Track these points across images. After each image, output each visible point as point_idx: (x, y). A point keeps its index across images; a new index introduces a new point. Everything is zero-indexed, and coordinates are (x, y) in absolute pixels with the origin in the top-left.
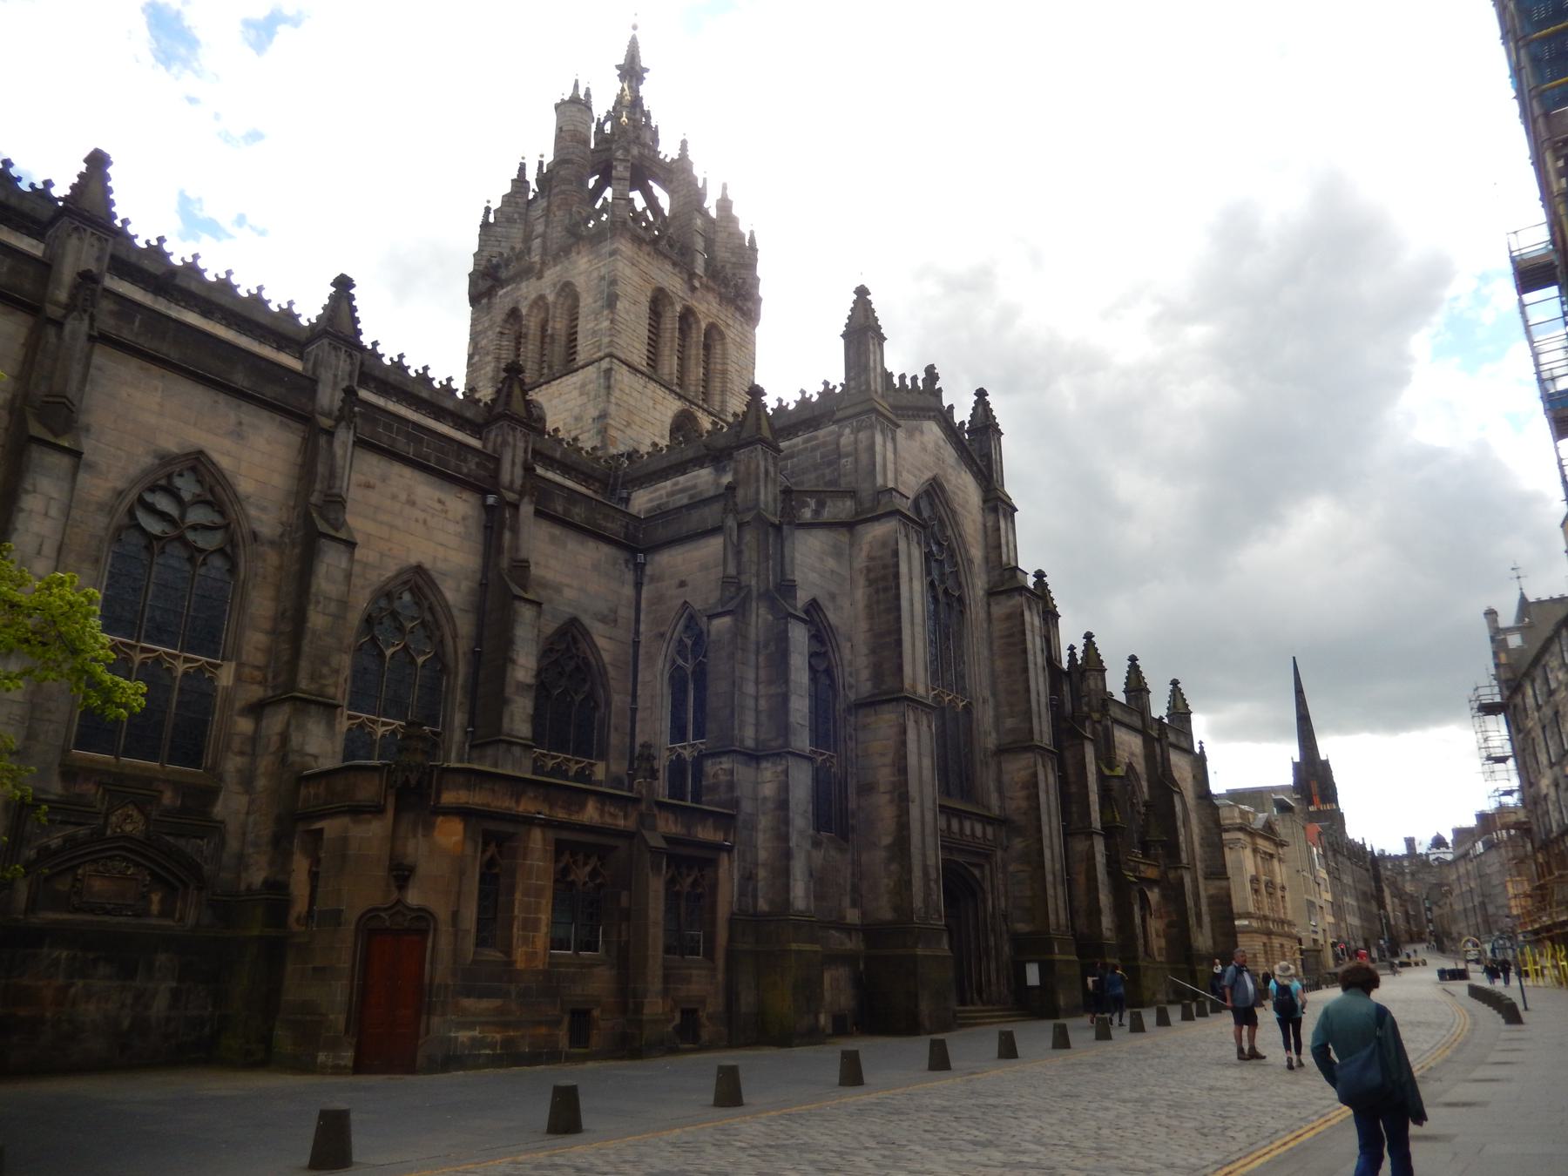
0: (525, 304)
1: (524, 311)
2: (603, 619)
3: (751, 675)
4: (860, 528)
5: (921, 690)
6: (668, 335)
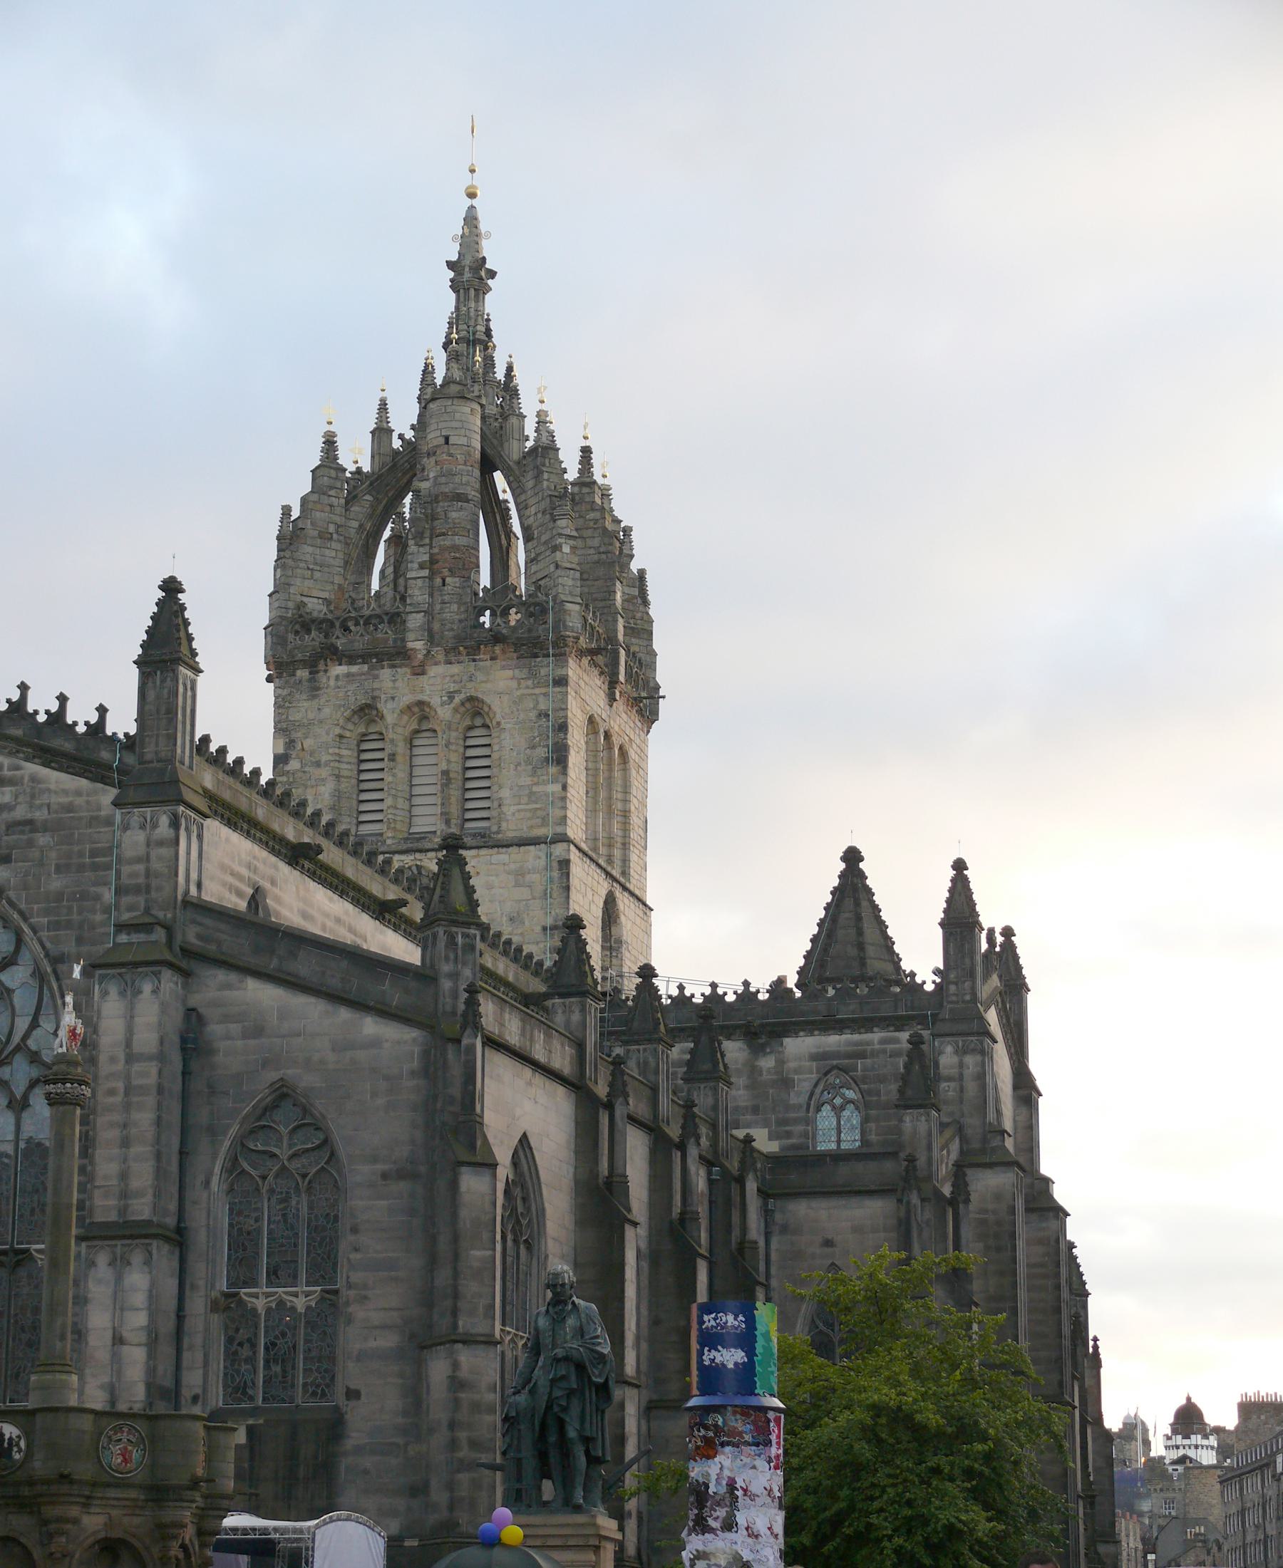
0: (390, 705)
1: (390, 718)
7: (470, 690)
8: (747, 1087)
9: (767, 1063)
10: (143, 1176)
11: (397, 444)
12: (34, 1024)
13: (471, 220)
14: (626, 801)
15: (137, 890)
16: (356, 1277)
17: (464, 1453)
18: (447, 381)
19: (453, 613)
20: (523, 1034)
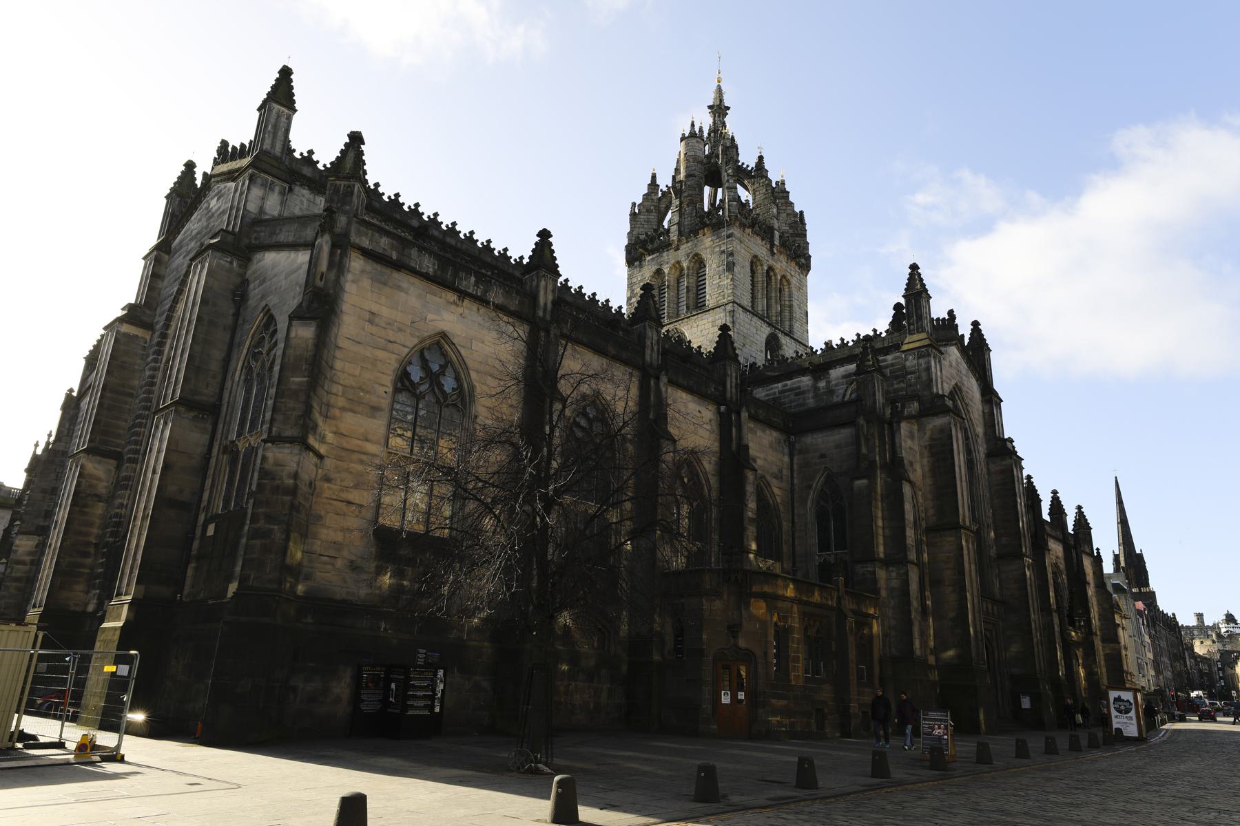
1: (666, 271)
2: (776, 477)
3: (880, 514)
4: (924, 419)
5: (968, 523)
6: (760, 285)
7: (697, 250)
8: (813, 398)
9: (822, 384)
13: (719, 91)
17: (261, 524)
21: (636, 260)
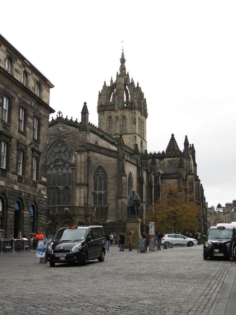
1: (113, 118)
7: (123, 114)
9: (162, 162)
10: (83, 177)
11: (113, 83)
12: (69, 159)
13: (123, 53)
14: (143, 128)
15: (81, 142)
16: (110, 190)
17: (123, 211)
18: (120, 74)
19: (121, 104)
20: (130, 159)
21: (102, 111)
